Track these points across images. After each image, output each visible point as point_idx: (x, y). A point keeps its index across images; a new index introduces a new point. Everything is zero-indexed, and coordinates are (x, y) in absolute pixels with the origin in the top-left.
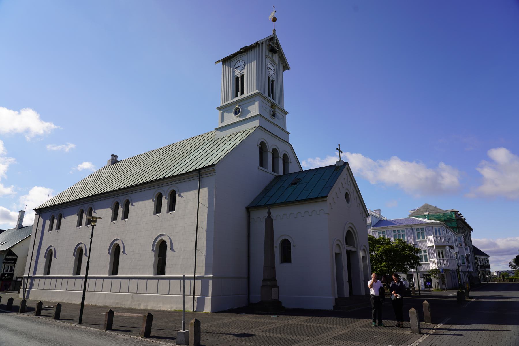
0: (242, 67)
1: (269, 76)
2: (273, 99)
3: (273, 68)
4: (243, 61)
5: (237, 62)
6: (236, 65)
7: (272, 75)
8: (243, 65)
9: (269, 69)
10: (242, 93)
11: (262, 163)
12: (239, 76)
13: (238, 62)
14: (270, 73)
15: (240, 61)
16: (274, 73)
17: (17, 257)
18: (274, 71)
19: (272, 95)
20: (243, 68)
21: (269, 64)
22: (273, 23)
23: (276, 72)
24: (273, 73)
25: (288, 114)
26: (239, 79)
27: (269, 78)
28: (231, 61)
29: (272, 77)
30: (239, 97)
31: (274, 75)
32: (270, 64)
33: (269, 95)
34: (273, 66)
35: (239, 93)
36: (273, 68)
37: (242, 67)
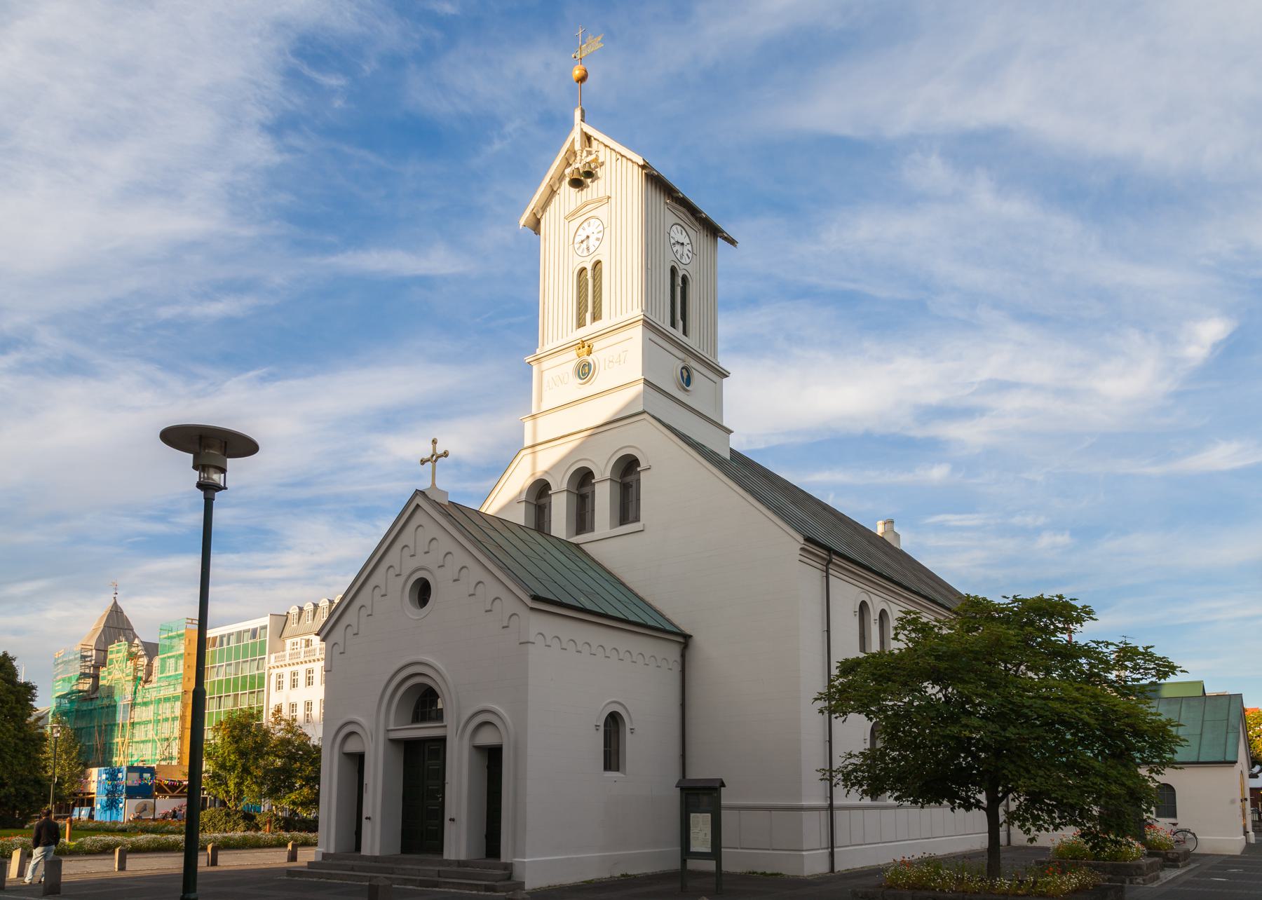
1: (676, 266)
2: (685, 333)
3: (686, 241)
6: (578, 233)
7: (683, 261)
8: (601, 232)
9: (674, 244)
10: (596, 317)
12: (589, 267)
13: (585, 225)
15: (592, 221)
16: (690, 255)
18: (691, 250)
20: (599, 242)
21: (674, 227)
24: (687, 255)
25: (727, 376)
27: (673, 271)
31: (688, 261)
32: (679, 228)
33: (673, 324)
34: (687, 234)
35: (588, 316)
36: (686, 241)
37: (598, 239)
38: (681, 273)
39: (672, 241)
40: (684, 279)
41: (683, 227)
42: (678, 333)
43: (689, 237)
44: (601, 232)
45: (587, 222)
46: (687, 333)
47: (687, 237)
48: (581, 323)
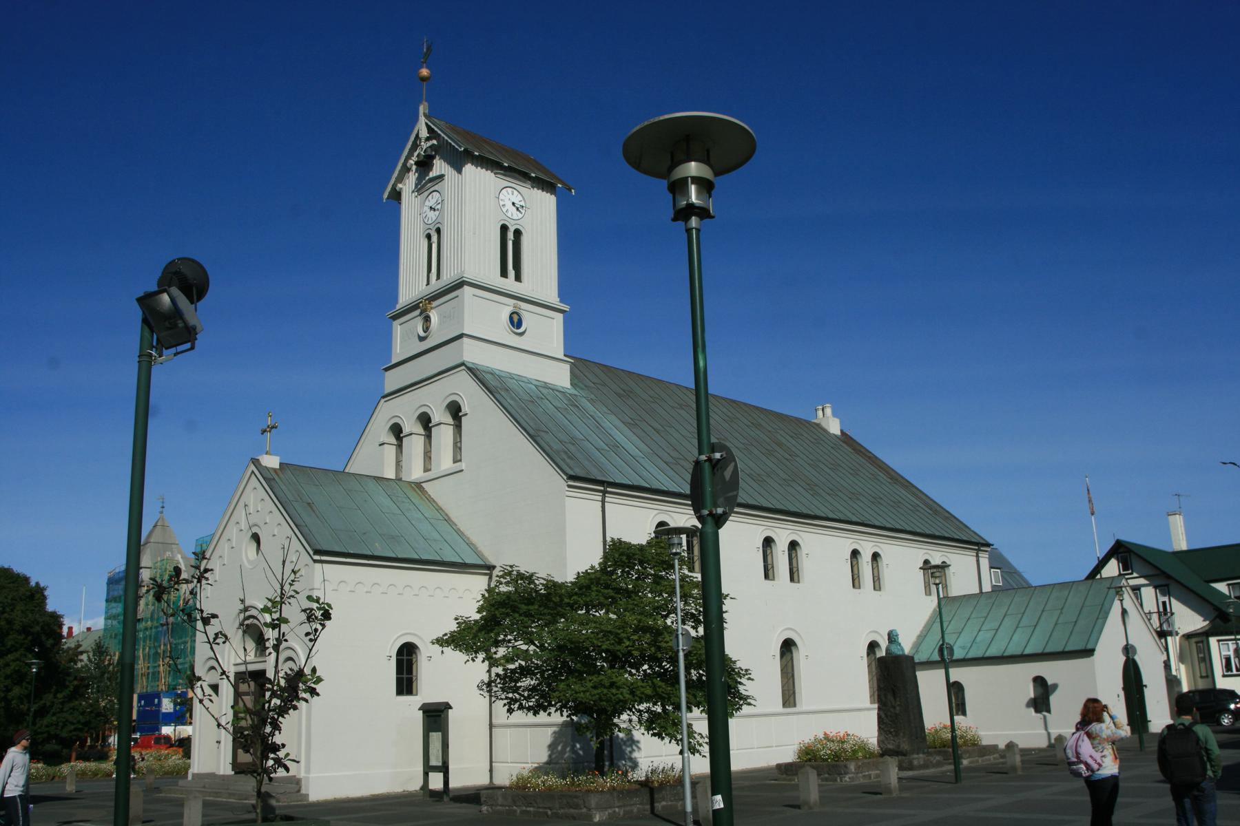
2: (518, 278)
7: (515, 217)
14: (509, 215)
15: (434, 193)
21: (504, 191)
27: (504, 229)
29: (516, 222)
30: (435, 285)
31: (520, 216)
32: (510, 190)
33: (504, 273)
38: (512, 229)
39: (502, 203)
40: (518, 233)
42: (509, 284)
43: (522, 195)
45: (431, 196)
46: (522, 280)
47: (519, 195)
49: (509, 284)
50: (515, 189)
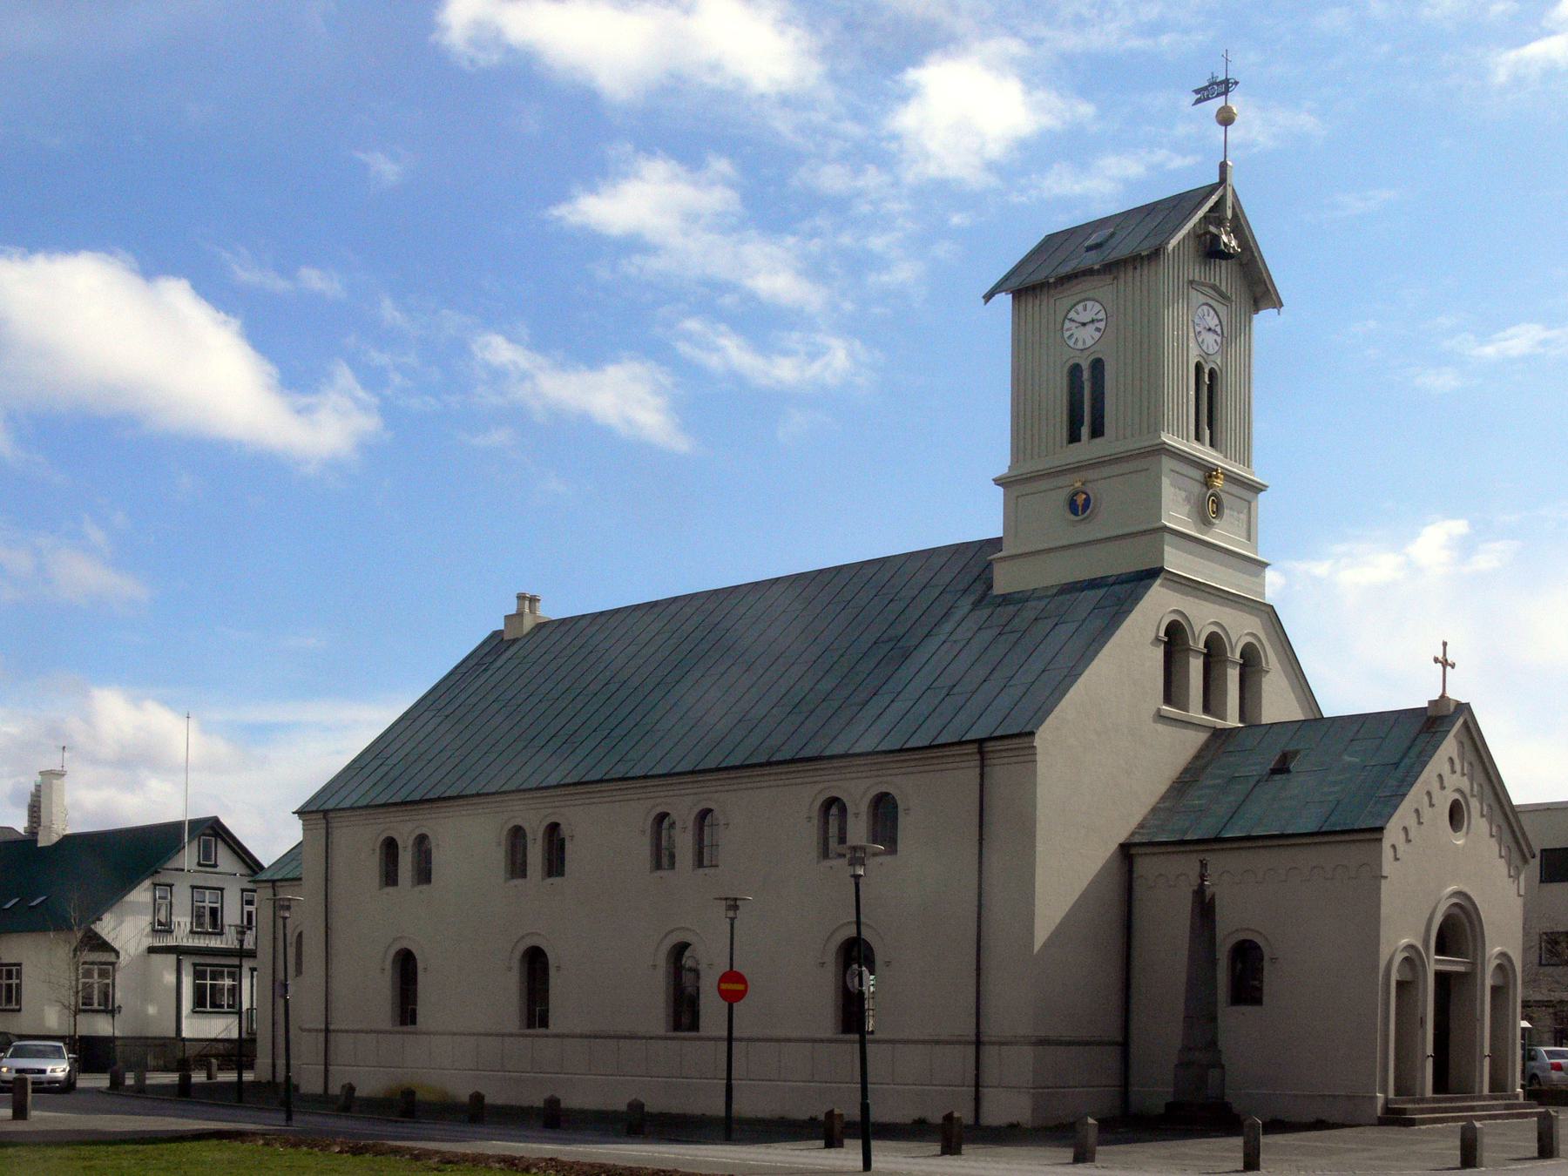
0: (1098, 330)
4: (1098, 307)
5: (1075, 305)
8: (1101, 320)
10: (1097, 431)
11: (1172, 690)
12: (1085, 365)
13: (1080, 307)
14: (1205, 348)
15: (1089, 304)
17: (117, 953)
19: (1207, 432)
22: (1224, 128)
23: (1225, 334)
26: (1086, 375)
28: (1053, 296)
34: (1216, 312)
35: (1085, 431)
37: (1098, 330)
40: (1212, 373)
41: (1211, 306)
42: (1204, 452)
43: (1218, 316)
44: (1101, 320)
47: (1215, 317)
48: (1074, 437)
49: (1204, 452)
50: (1214, 310)
